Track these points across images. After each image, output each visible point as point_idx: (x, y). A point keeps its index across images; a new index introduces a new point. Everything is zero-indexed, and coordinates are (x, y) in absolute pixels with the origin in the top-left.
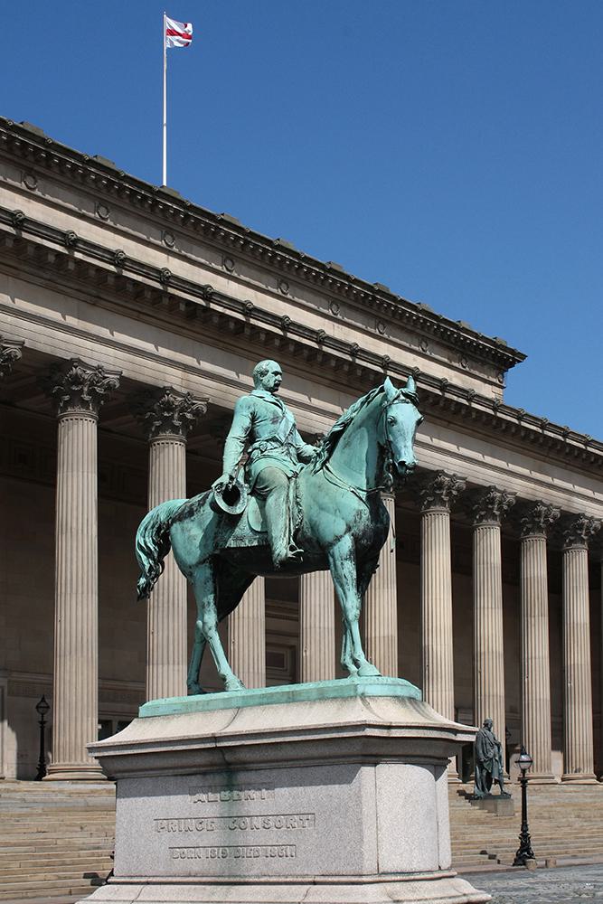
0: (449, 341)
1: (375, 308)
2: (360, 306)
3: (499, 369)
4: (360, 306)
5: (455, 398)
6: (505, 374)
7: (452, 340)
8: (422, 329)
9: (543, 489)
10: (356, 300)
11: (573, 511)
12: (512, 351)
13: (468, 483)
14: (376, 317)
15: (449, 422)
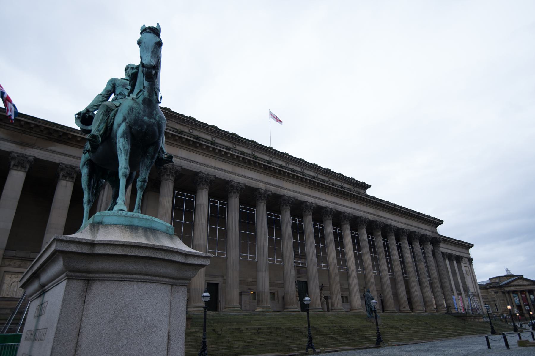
0: (349, 182)
1: (328, 174)
2: (324, 174)
3: (364, 190)
4: (324, 174)
5: (346, 191)
6: (366, 191)
7: (350, 182)
8: (341, 180)
9: (378, 217)
10: (322, 173)
11: (388, 224)
12: (368, 185)
13: (354, 216)
14: (329, 177)
15: (346, 198)
